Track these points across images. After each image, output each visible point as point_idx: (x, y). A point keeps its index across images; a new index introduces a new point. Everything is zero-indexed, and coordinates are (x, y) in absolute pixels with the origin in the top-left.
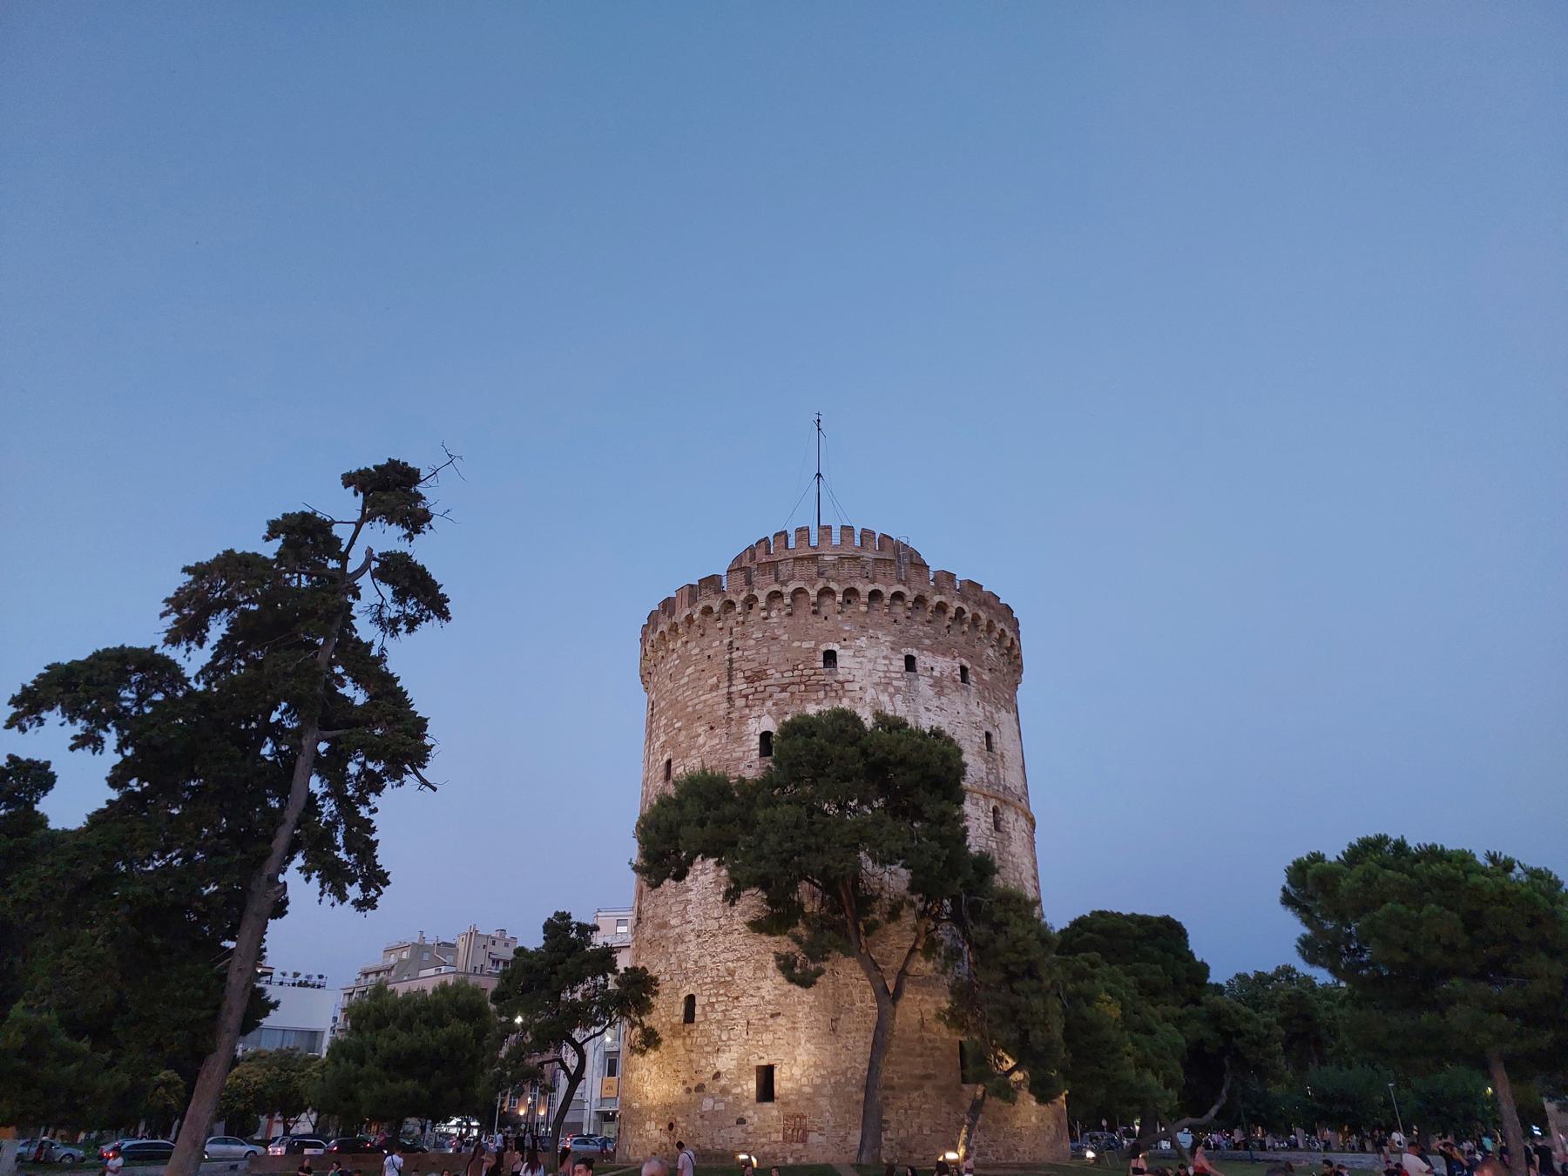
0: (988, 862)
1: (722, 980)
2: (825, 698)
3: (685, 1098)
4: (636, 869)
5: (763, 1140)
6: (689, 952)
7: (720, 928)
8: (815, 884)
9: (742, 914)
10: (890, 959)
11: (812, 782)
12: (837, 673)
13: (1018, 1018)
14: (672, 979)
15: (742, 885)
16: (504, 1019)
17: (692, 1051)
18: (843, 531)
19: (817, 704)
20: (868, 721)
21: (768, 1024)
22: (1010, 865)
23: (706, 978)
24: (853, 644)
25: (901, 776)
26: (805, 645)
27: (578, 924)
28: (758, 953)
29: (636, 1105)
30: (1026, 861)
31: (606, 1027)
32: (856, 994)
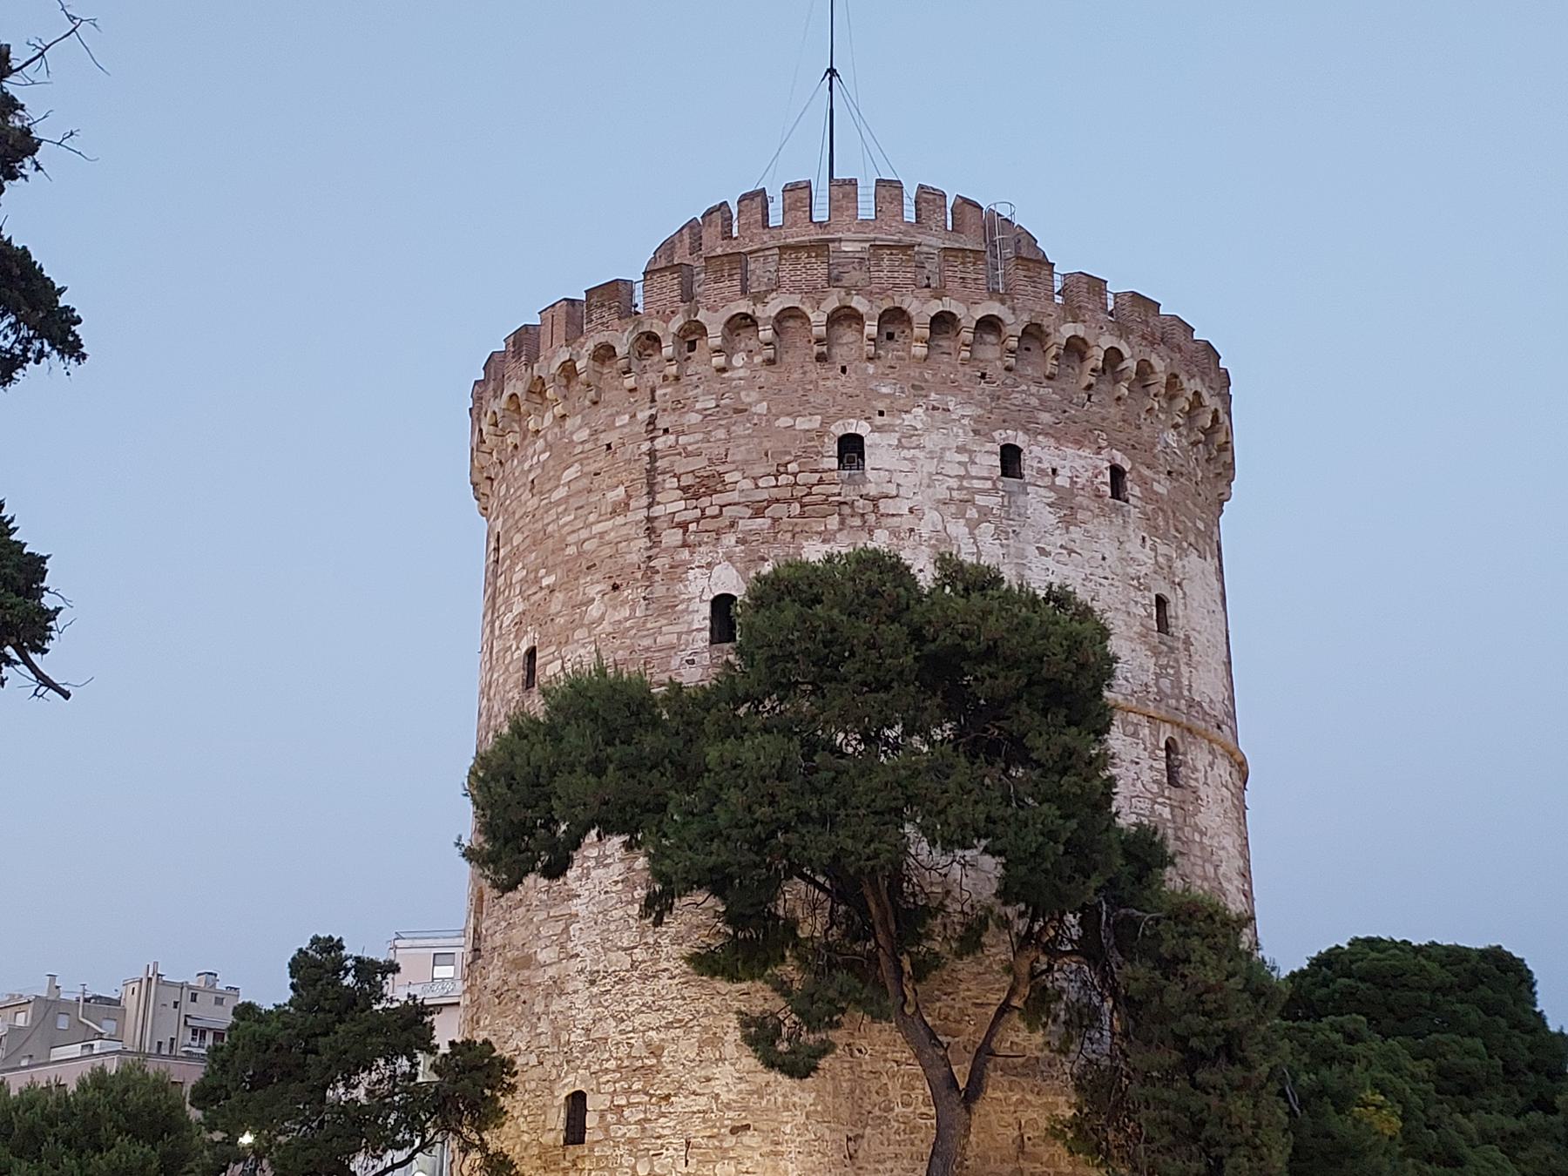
0: (1153, 844)
1: (639, 1063)
2: (840, 530)
4: (470, 855)
7: (634, 966)
8: (821, 887)
9: (677, 940)
10: (962, 1026)
11: (813, 692)
12: (865, 481)
15: (678, 887)
16: (218, 1136)
18: (883, 191)
19: (824, 541)
20: (926, 575)
21: (725, 1145)
23: (608, 1060)
24: (899, 421)
26: (802, 424)
27: (358, 959)
28: (707, 1013)
31: (415, 1152)
32: (895, 1091)
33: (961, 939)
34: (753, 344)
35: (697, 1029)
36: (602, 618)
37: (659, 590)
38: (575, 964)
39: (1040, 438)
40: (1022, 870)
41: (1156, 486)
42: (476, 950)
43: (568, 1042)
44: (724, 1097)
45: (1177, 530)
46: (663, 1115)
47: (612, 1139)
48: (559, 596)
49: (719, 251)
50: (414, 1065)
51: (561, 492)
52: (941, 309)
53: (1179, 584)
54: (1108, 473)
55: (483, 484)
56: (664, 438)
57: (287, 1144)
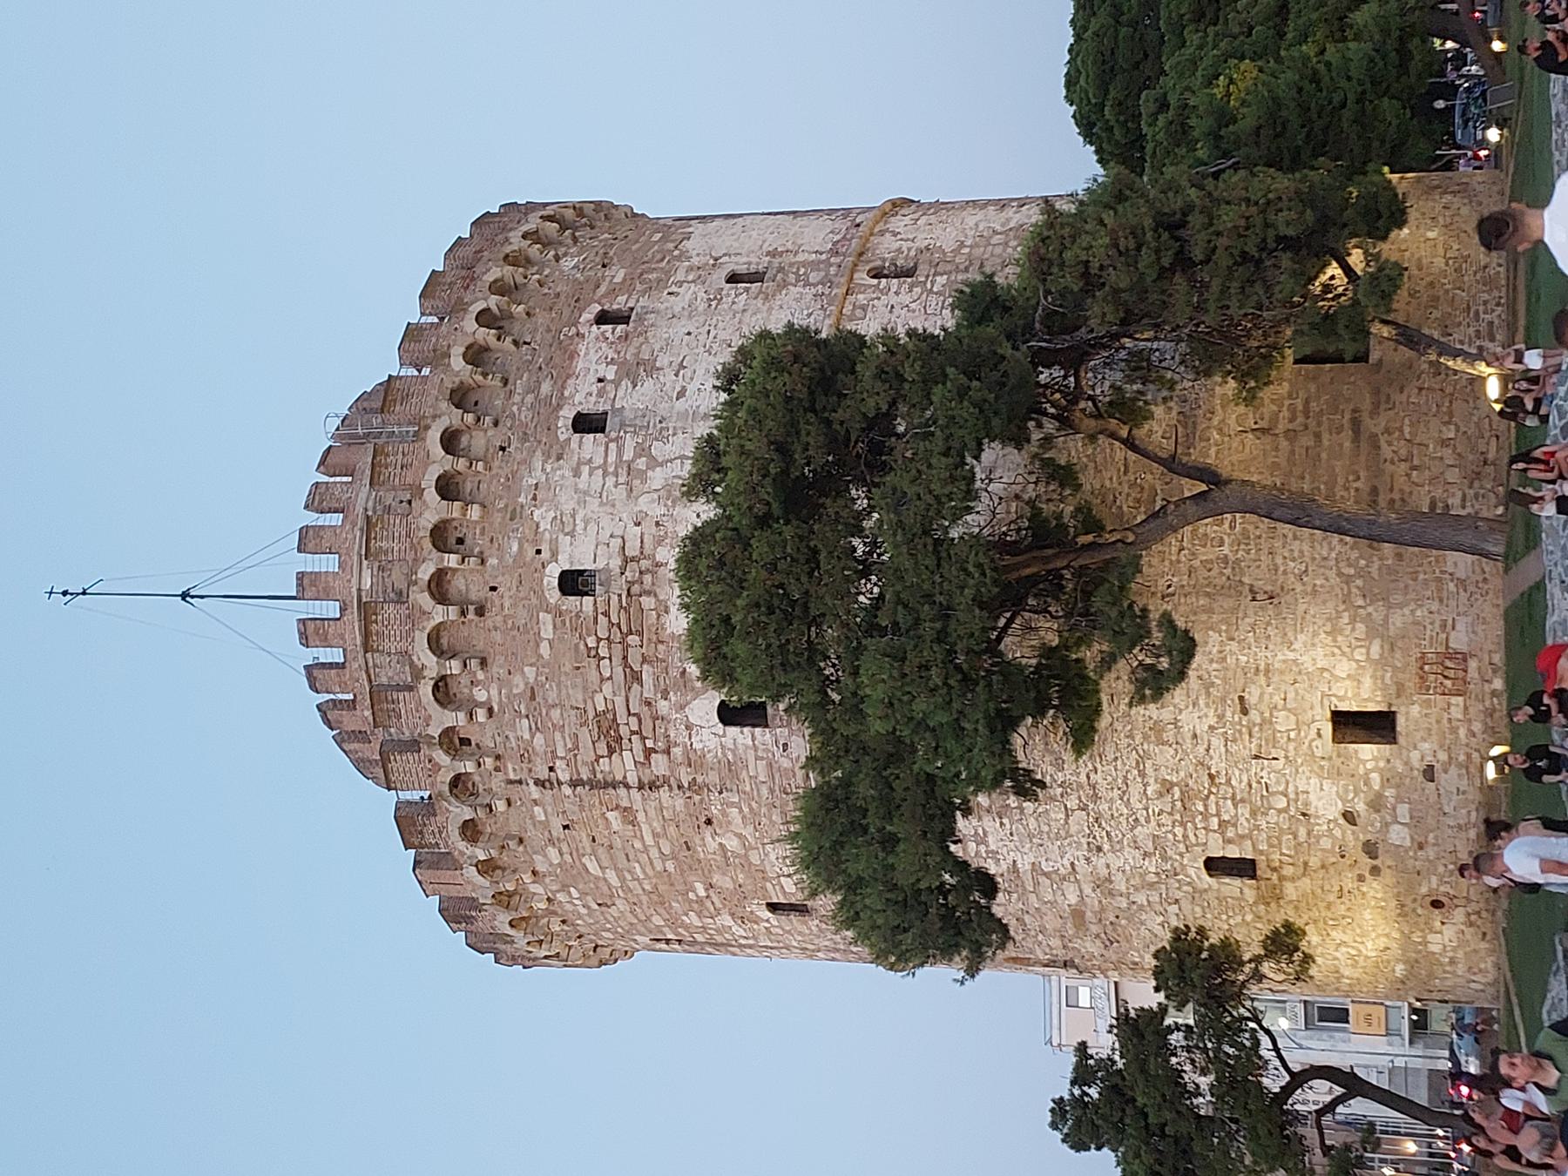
0: (972, 295)
1: (1179, 804)
2: (655, 595)
3: (1388, 877)
4: (972, 971)
5: (1462, 732)
6: (1128, 868)
8: (1010, 621)
10: (1146, 486)
12: (607, 570)
13: (1254, 252)
14: (1177, 901)
17: (1306, 864)
20: (703, 511)
21: (1258, 721)
22: (978, 252)
23: (1175, 835)
24: (547, 535)
25: (811, 453)
26: (547, 632)
27: (1073, 1083)
28: (1131, 736)
29: (1400, 970)
30: (971, 221)
31: (1262, 1027)
33: (1062, 486)
34: (465, 680)
35: (1146, 747)
36: (739, 836)
37: (713, 778)
38: (1081, 865)
39: (566, 393)
40: (996, 422)
41: (618, 279)
42: (1065, 965)
43: (1157, 874)
44: (1212, 721)
45: (662, 260)
46: (1229, 782)
47: (1251, 831)
48: (716, 879)
49: (368, 713)
50: (1178, 1028)
51: (611, 876)
52: (433, 489)
53: (716, 260)
54: (604, 327)
55: (601, 955)
56: (559, 771)
57: (1253, 1154)
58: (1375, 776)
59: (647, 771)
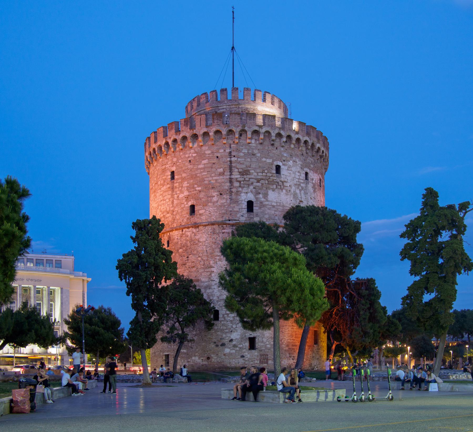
37: (234, 197)
58: (242, 346)
59: (235, 181)
